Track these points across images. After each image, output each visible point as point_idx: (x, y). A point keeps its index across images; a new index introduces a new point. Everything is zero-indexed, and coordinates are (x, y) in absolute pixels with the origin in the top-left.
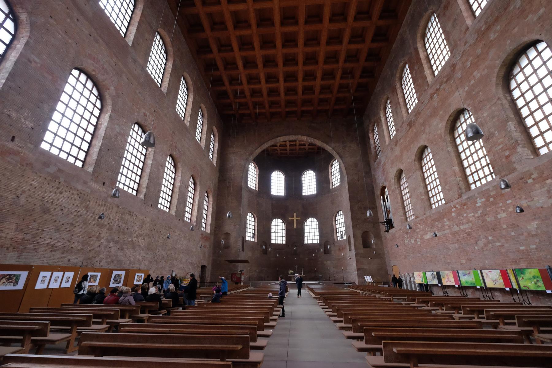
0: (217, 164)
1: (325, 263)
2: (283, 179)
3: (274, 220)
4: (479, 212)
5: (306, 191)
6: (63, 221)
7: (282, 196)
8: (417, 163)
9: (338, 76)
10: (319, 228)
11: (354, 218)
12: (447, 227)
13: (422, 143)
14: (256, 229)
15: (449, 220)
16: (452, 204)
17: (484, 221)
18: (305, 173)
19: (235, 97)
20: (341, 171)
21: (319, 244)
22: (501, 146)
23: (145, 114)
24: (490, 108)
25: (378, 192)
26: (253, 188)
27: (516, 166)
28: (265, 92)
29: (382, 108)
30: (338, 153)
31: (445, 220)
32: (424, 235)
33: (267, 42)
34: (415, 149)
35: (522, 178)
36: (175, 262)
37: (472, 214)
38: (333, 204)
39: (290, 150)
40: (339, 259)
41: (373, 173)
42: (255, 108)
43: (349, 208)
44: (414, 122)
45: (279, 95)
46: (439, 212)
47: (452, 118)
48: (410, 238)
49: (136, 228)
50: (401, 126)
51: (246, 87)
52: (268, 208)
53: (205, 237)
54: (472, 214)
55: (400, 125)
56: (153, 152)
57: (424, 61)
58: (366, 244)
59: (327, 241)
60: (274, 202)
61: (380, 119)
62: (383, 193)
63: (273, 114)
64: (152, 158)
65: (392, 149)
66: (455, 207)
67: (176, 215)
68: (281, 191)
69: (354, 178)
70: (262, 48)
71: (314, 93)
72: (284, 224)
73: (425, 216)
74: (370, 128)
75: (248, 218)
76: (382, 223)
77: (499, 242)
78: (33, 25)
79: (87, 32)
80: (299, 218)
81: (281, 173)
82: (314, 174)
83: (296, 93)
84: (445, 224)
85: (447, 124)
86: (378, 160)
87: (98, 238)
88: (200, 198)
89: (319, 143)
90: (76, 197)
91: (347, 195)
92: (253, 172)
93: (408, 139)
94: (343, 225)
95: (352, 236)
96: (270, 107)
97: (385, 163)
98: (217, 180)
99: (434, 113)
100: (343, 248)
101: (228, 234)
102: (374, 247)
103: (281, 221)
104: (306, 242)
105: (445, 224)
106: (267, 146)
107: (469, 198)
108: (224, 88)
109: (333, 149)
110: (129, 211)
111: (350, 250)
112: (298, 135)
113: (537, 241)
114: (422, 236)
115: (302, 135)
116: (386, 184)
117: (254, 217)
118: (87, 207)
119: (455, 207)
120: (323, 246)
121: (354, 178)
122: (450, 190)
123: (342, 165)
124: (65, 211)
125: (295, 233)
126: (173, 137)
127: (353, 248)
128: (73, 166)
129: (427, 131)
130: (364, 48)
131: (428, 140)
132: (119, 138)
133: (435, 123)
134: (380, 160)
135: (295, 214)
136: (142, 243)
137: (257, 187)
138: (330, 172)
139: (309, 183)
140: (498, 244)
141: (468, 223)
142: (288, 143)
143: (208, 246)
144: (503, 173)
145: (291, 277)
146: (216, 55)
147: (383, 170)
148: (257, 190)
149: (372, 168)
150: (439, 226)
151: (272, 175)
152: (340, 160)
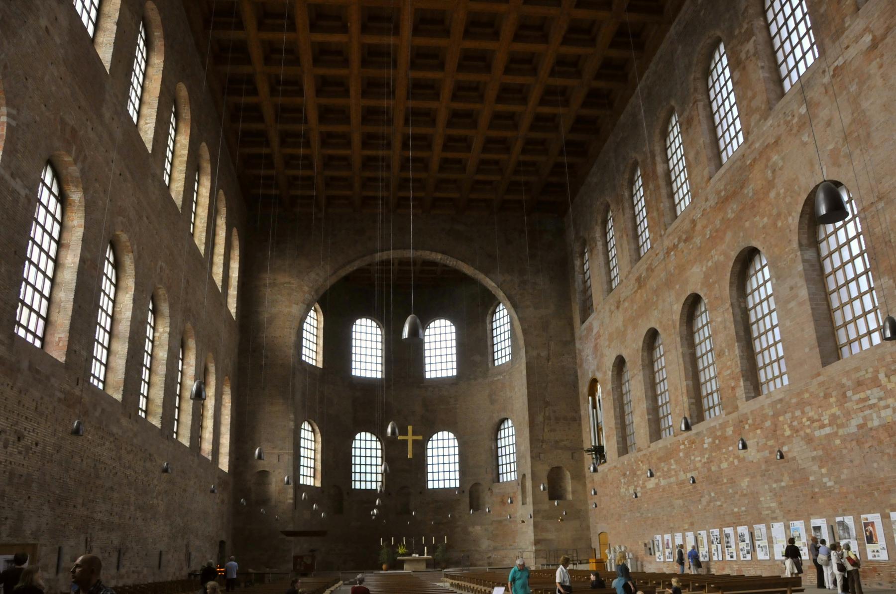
1: (471, 529)
2: (379, 338)
3: (358, 437)
4: (706, 456)
5: (433, 367)
8: (645, 354)
10: (460, 454)
11: (534, 440)
12: (673, 473)
14: (319, 457)
15: (676, 461)
17: (709, 470)
20: (512, 330)
21: (461, 489)
22: (729, 372)
23: (161, 268)
25: (584, 389)
26: (311, 362)
27: (739, 403)
29: (600, 221)
30: (510, 298)
31: (672, 461)
32: (646, 481)
35: (742, 422)
37: (699, 458)
38: (492, 402)
40: (500, 522)
41: (578, 345)
43: (527, 418)
44: (644, 280)
46: (666, 446)
47: (689, 302)
48: (628, 484)
49: (156, 482)
50: (626, 277)
52: (343, 405)
54: (699, 458)
55: (625, 273)
56: (166, 335)
59: (477, 484)
61: (594, 240)
62: (592, 392)
64: (166, 348)
65: (611, 312)
66: (684, 444)
67: (190, 445)
69: (539, 355)
72: (379, 446)
73: (650, 450)
74: (577, 248)
75: (303, 434)
76: (588, 451)
77: (720, 500)
78: (89, 209)
79: (118, 173)
80: (420, 438)
81: (374, 324)
82: (453, 329)
84: (672, 467)
85: (683, 308)
86: (587, 323)
89: (467, 269)
91: (525, 391)
93: (635, 308)
94: (512, 449)
97: (598, 336)
101: (264, 474)
102: (570, 497)
103: (374, 438)
104: (430, 486)
105: (672, 467)
106: (351, 270)
107: (697, 434)
109: (500, 286)
110: (150, 455)
111: (523, 504)
112: (423, 249)
113: (746, 502)
114: (643, 484)
115: (432, 251)
116: (599, 376)
117: (313, 431)
119: (684, 444)
120: (467, 494)
121: (539, 355)
123: (517, 323)
125: (405, 466)
126: (187, 293)
129: (660, 307)
131: (661, 322)
134: (591, 324)
135: (410, 428)
137: (320, 358)
141: (695, 470)
145: (403, 562)
147: (596, 346)
148: (320, 365)
150: (665, 469)
152: (512, 311)
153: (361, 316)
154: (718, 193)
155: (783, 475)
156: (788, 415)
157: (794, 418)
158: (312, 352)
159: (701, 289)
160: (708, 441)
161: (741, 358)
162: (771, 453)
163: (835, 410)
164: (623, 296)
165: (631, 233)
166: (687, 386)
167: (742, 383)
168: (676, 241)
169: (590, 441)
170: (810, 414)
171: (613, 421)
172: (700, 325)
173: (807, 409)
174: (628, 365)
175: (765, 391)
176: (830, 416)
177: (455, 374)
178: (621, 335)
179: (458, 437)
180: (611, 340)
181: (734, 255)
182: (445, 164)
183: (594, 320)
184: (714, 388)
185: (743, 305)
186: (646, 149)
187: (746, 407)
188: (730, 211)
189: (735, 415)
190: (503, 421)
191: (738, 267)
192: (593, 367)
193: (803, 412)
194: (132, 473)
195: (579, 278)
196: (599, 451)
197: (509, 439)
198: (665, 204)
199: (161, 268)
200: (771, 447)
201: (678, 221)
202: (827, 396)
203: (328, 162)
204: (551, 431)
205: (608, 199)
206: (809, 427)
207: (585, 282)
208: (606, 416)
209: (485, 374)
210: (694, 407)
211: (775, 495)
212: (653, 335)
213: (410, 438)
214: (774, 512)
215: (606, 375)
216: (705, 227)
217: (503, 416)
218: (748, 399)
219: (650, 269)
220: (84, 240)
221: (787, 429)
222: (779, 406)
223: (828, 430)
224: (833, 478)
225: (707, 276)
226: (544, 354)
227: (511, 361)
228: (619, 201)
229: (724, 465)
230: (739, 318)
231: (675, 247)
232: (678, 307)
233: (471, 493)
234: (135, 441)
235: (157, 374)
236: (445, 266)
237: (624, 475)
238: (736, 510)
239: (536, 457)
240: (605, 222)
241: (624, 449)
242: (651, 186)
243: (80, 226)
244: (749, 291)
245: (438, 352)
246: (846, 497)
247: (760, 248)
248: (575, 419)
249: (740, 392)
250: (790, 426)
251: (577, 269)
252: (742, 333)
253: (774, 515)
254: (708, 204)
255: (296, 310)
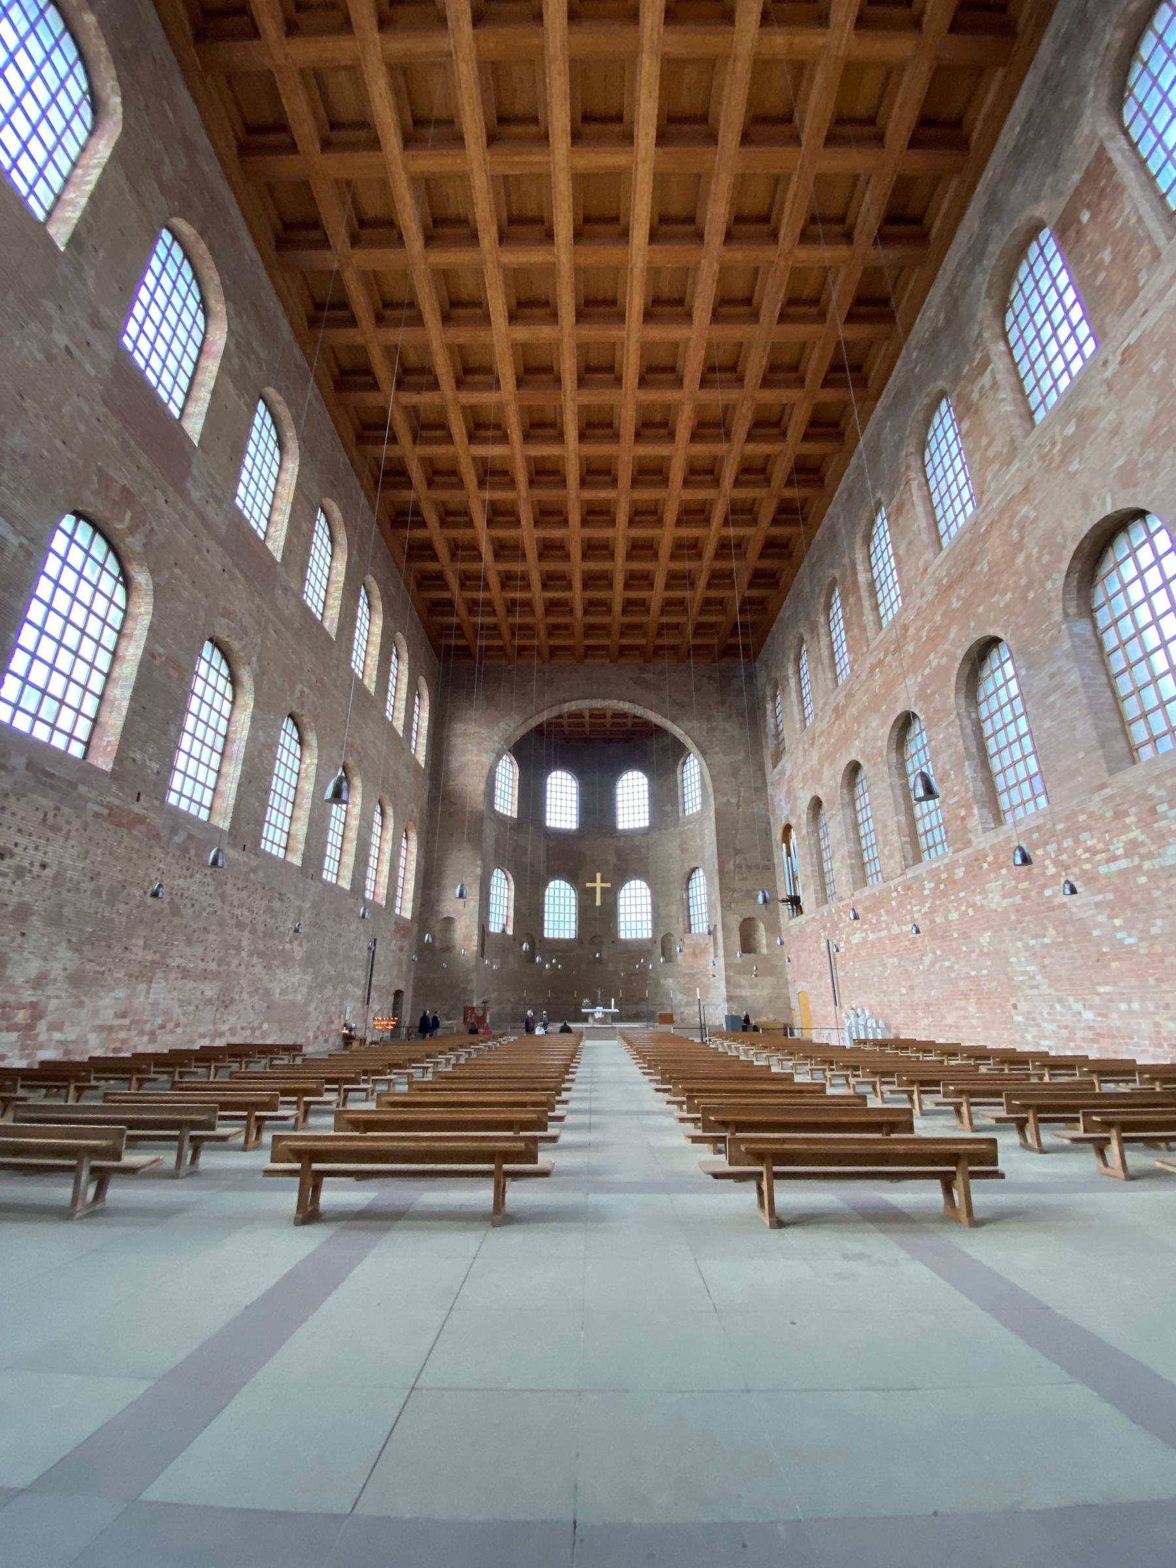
0: (426, 762)
1: (662, 981)
2: (574, 791)
3: (551, 884)
6: (195, 926)
7: (570, 831)
9: (702, 583)
11: (725, 889)
13: (854, 756)
15: (887, 912)
16: (892, 884)
17: (933, 921)
18: (625, 777)
19: (471, 612)
20: (702, 780)
21: (653, 941)
23: (302, 692)
24: (947, 727)
27: (971, 836)
28: (539, 608)
29: (792, 656)
30: (698, 745)
33: (541, 427)
34: (842, 764)
36: (349, 987)
38: (683, 851)
39: (591, 725)
41: (770, 791)
42: (510, 611)
45: (571, 612)
47: (899, 724)
51: (497, 595)
53: (401, 928)
56: (314, 767)
57: (864, 593)
58: (748, 945)
60: (552, 844)
61: (786, 678)
62: (786, 837)
63: (554, 651)
64: (313, 780)
65: (805, 751)
68: (569, 818)
70: (537, 523)
71: (648, 611)
74: (769, 692)
75: (494, 881)
79: (219, 567)
80: (608, 885)
82: (646, 780)
83: (609, 611)
86: (779, 767)
87: (238, 948)
88: (394, 844)
89: (655, 718)
90: (209, 880)
91: (714, 838)
92: (508, 774)
95: (719, 927)
96: (550, 634)
97: (792, 778)
98: (425, 797)
99: (873, 706)
100: (704, 951)
101: (449, 921)
102: (764, 951)
108: (446, 595)
115: (620, 699)
116: (793, 821)
118: (223, 896)
122: (891, 857)
123: (706, 770)
124: (197, 907)
125: (597, 917)
127: (721, 952)
128: (64, 755)
129: (862, 735)
130: (756, 535)
132: (266, 752)
133: (874, 724)
135: (598, 876)
136: (299, 952)
138: (679, 777)
139: (632, 798)
140: (947, 964)
142: (587, 715)
143: (407, 948)
144: (958, 845)
146: (419, 492)
148: (515, 815)
149: (769, 778)
151: (549, 780)
153: (555, 769)
154: (938, 582)
155: (1046, 928)
156: (1051, 848)
157: (1060, 850)
158: (507, 802)
159: (915, 704)
160: (929, 885)
161: (974, 780)
162: (1024, 898)
163: (1136, 834)
164: (818, 731)
165: (827, 661)
166: (899, 822)
167: (976, 811)
168: (882, 656)
169: (784, 892)
170: (1090, 843)
171: (809, 869)
172: (913, 751)
173: (1084, 836)
174: (825, 805)
175: (1009, 818)
176: (1126, 843)
177: (646, 823)
178: (816, 775)
179: (651, 886)
180: (805, 781)
181: (961, 653)
182: (629, 604)
183: (786, 763)
184: (935, 823)
185: (973, 716)
186: (846, 560)
187: (982, 841)
188: (954, 600)
189: (968, 851)
190: (694, 870)
191: (967, 668)
192: (785, 813)
193: (1077, 841)
194: (246, 913)
195: (771, 722)
196: (795, 901)
197: (701, 890)
198: (869, 617)
199: (302, 692)
200: (1025, 890)
201: (883, 633)
202: (1119, 815)
203: (511, 606)
204: (744, 879)
205: (802, 630)
206: (1088, 860)
207: (777, 726)
208: (802, 863)
209: (676, 825)
210: (908, 847)
211: (1034, 955)
212: (854, 768)
213: (598, 885)
214: (1033, 978)
215: (801, 819)
216: (919, 629)
217: (694, 865)
218: (985, 830)
219: (850, 695)
220: (151, 629)
221: (1051, 866)
222: (1035, 836)
223: (1123, 864)
224: (1134, 932)
225: (923, 688)
226: (734, 800)
227: (702, 810)
228: (814, 628)
229: (954, 916)
230: (969, 731)
231: (881, 662)
232: (886, 731)
233: (663, 942)
234: (252, 876)
235: (301, 808)
236: (635, 717)
237: (824, 928)
238: (973, 973)
239: (726, 907)
240: (798, 658)
241: (823, 898)
242: (851, 600)
243: (147, 613)
244: (981, 697)
245: (631, 803)
246: (1162, 961)
247: (1001, 635)
248: (768, 868)
249: (974, 822)
250: (1056, 862)
251: (769, 713)
252: (974, 750)
253: (1034, 983)
254: (925, 599)
255: (486, 759)
